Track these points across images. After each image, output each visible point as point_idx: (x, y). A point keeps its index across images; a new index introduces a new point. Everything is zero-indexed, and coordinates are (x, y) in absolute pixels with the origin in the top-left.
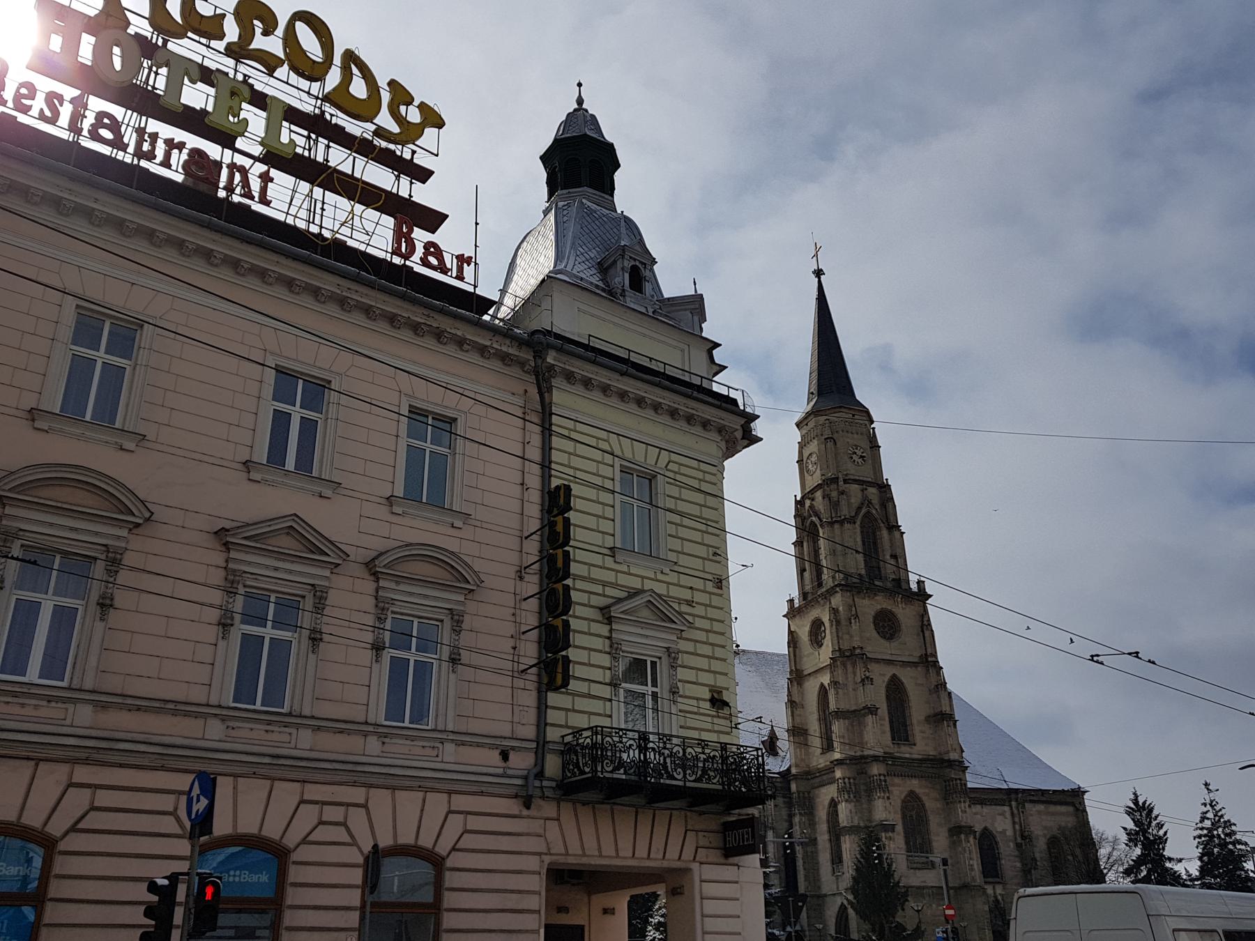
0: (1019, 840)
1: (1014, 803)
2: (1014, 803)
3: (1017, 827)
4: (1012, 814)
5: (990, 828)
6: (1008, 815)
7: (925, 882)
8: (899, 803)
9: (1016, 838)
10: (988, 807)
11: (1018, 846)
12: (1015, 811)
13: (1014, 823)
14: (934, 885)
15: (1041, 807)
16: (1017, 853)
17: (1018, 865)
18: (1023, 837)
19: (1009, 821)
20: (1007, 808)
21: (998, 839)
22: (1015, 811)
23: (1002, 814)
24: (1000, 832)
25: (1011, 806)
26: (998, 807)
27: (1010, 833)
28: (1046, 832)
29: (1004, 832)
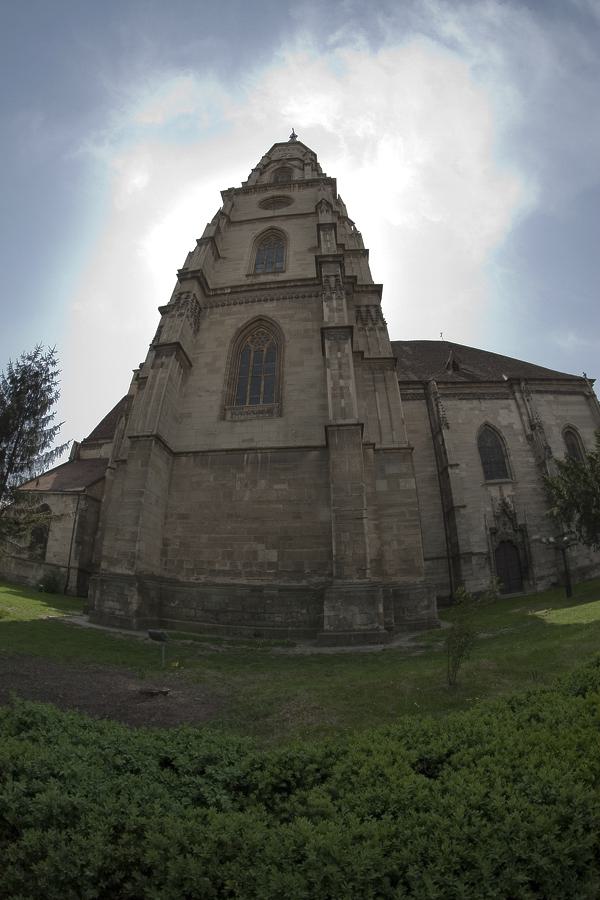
0: (529, 431)
1: (518, 395)
2: (518, 395)
3: (525, 418)
4: (518, 407)
5: (491, 421)
6: (513, 407)
7: (252, 440)
8: (231, 332)
9: (525, 431)
10: (489, 402)
11: (529, 438)
12: (521, 402)
13: (521, 415)
14: (271, 445)
15: (551, 397)
16: (528, 447)
17: (532, 460)
18: (533, 427)
19: (515, 414)
20: (511, 402)
21: (504, 434)
22: (521, 402)
23: (507, 407)
24: (506, 427)
25: (515, 399)
26: (499, 402)
27: (518, 426)
28: (558, 421)
29: (510, 426)
